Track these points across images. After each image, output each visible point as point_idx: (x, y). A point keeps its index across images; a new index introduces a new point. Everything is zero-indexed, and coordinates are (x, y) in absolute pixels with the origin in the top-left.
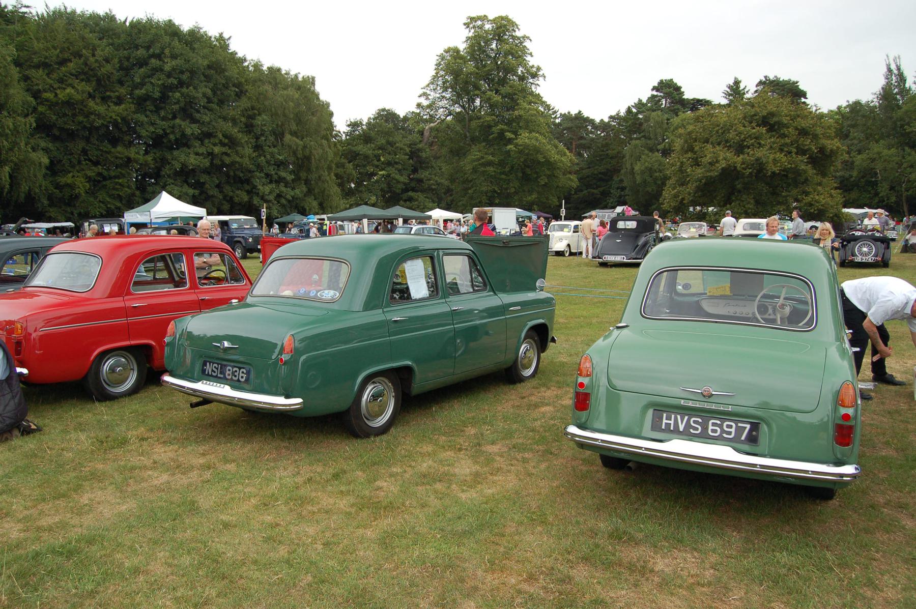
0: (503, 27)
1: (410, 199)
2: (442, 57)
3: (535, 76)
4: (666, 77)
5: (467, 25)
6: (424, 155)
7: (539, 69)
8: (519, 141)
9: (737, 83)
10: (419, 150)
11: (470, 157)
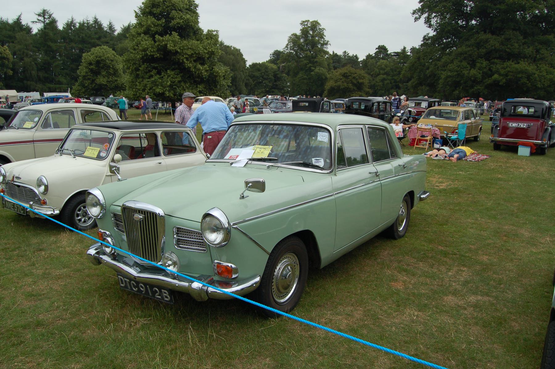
0: (315, 25)
1: (273, 92)
2: (290, 37)
3: (327, 44)
4: (381, 44)
5: (301, 24)
6: (278, 76)
7: (328, 41)
8: (316, 71)
9: (405, 48)
10: (277, 74)
11: (298, 76)
